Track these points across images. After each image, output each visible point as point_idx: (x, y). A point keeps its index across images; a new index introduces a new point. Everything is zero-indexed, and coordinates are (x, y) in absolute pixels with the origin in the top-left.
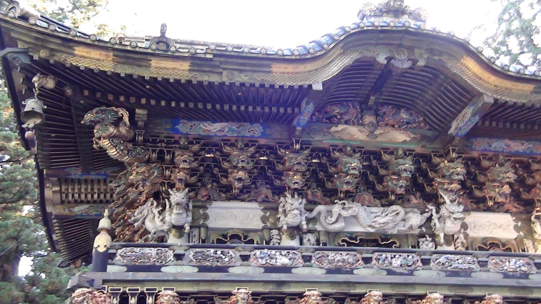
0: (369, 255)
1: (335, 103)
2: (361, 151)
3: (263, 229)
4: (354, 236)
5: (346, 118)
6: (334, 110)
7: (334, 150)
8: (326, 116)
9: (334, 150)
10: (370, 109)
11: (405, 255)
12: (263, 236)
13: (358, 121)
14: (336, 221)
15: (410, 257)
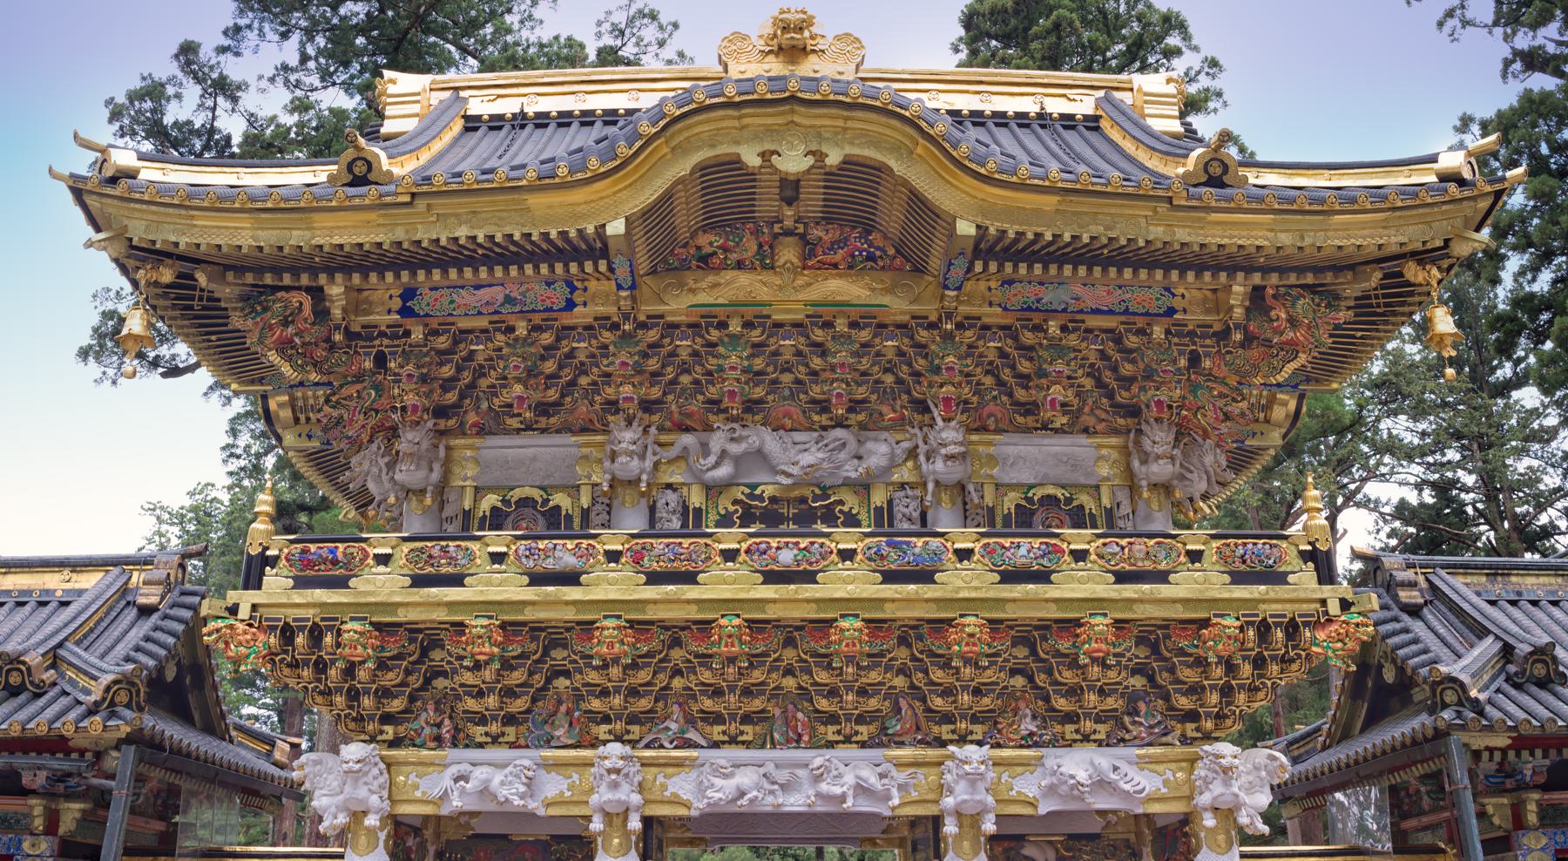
2: (763, 325)
4: (758, 492)
5: (734, 256)
7: (708, 325)
9: (708, 325)
10: (788, 233)
13: (762, 261)
14: (717, 465)
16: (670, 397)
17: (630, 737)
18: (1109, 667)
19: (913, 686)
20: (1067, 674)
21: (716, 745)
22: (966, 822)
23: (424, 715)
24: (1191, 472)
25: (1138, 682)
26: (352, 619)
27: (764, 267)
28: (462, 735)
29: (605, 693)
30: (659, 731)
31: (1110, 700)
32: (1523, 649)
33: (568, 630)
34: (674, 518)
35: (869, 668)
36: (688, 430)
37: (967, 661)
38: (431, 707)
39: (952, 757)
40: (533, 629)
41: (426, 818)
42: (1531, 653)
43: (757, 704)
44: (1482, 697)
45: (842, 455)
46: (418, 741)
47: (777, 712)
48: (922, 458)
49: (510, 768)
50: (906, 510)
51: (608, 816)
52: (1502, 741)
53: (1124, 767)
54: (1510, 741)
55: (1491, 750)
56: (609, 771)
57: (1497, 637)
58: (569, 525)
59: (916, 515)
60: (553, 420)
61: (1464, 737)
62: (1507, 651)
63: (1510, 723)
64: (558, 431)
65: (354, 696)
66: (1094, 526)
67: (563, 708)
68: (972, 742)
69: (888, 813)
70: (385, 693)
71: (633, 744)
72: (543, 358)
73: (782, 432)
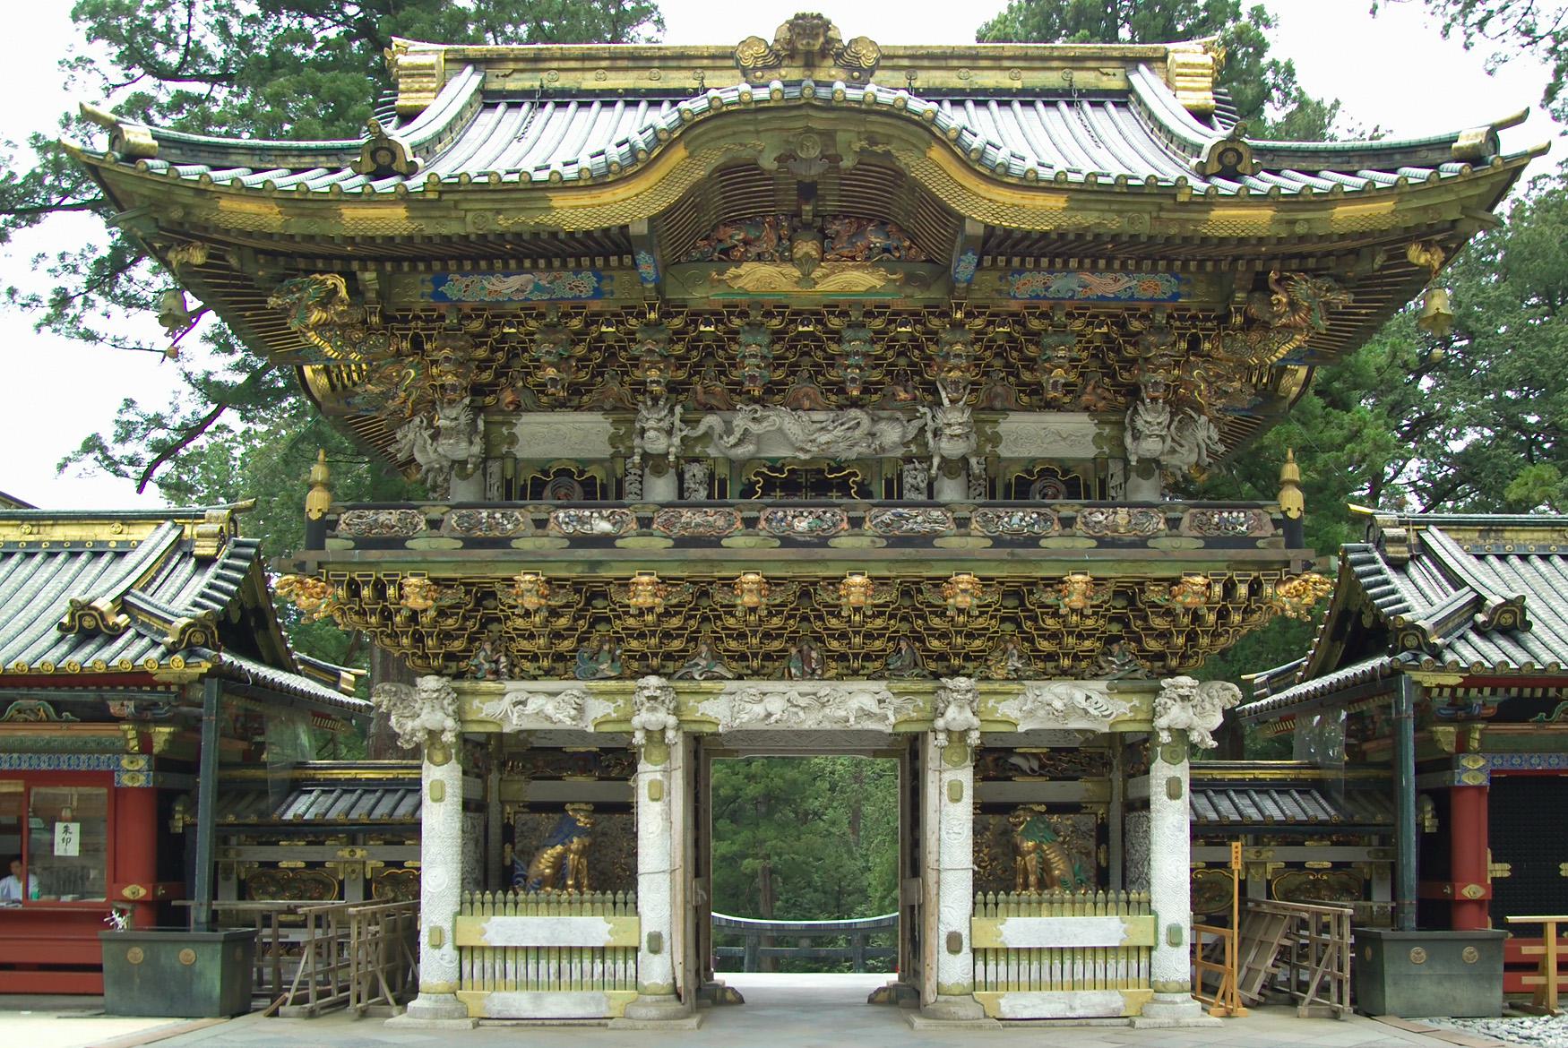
0: (754, 514)
1: (733, 222)
2: (782, 314)
3: (613, 457)
4: (778, 465)
5: (754, 251)
6: (731, 237)
7: (730, 314)
8: (721, 246)
9: (730, 314)
10: (807, 226)
11: (820, 511)
12: (614, 470)
13: (781, 254)
15: (828, 515)
16: (696, 378)
17: (666, 671)
18: (1088, 617)
19: (913, 631)
20: (1050, 621)
21: (740, 677)
22: (955, 737)
23: (482, 654)
24: (1182, 446)
25: (1115, 629)
26: (412, 575)
27: (783, 260)
28: (517, 670)
29: (642, 635)
30: (690, 667)
31: (1088, 644)
32: (1494, 600)
33: (608, 583)
34: (701, 489)
35: (874, 616)
36: (711, 409)
37: (960, 611)
38: (488, 646)
39: (945, 688)
40: (575, 583)
41: (489, 735)
42: (1501, 605)
43: (776, 645)
44: (1439, 641)
45: (857, 433)
46: (479, 675)
47: (794, 651)
48: (929, 435)
49: (562, 696)
50: (914, 482)
51: (649, 733)
52: (1454, 679)
53: (1095, 697)
54: (1461, 680)
55: (1441, 687)
56: (649, 698)
57: (1473, 590)
58: (604, 496)
59: (923, 485)
60: (585, 398)
61: (1417, 676)
62: (1478, 602)
63: (1463, 665)
64: (590, 409)
65: (418, 639)
66: (1088, 497)
67: (606, 647)
68: (963, 675)
69: (890, 730)
70: (448, 636)
71: (669, 676)
72: (575, 343)
73: (800, 412)
